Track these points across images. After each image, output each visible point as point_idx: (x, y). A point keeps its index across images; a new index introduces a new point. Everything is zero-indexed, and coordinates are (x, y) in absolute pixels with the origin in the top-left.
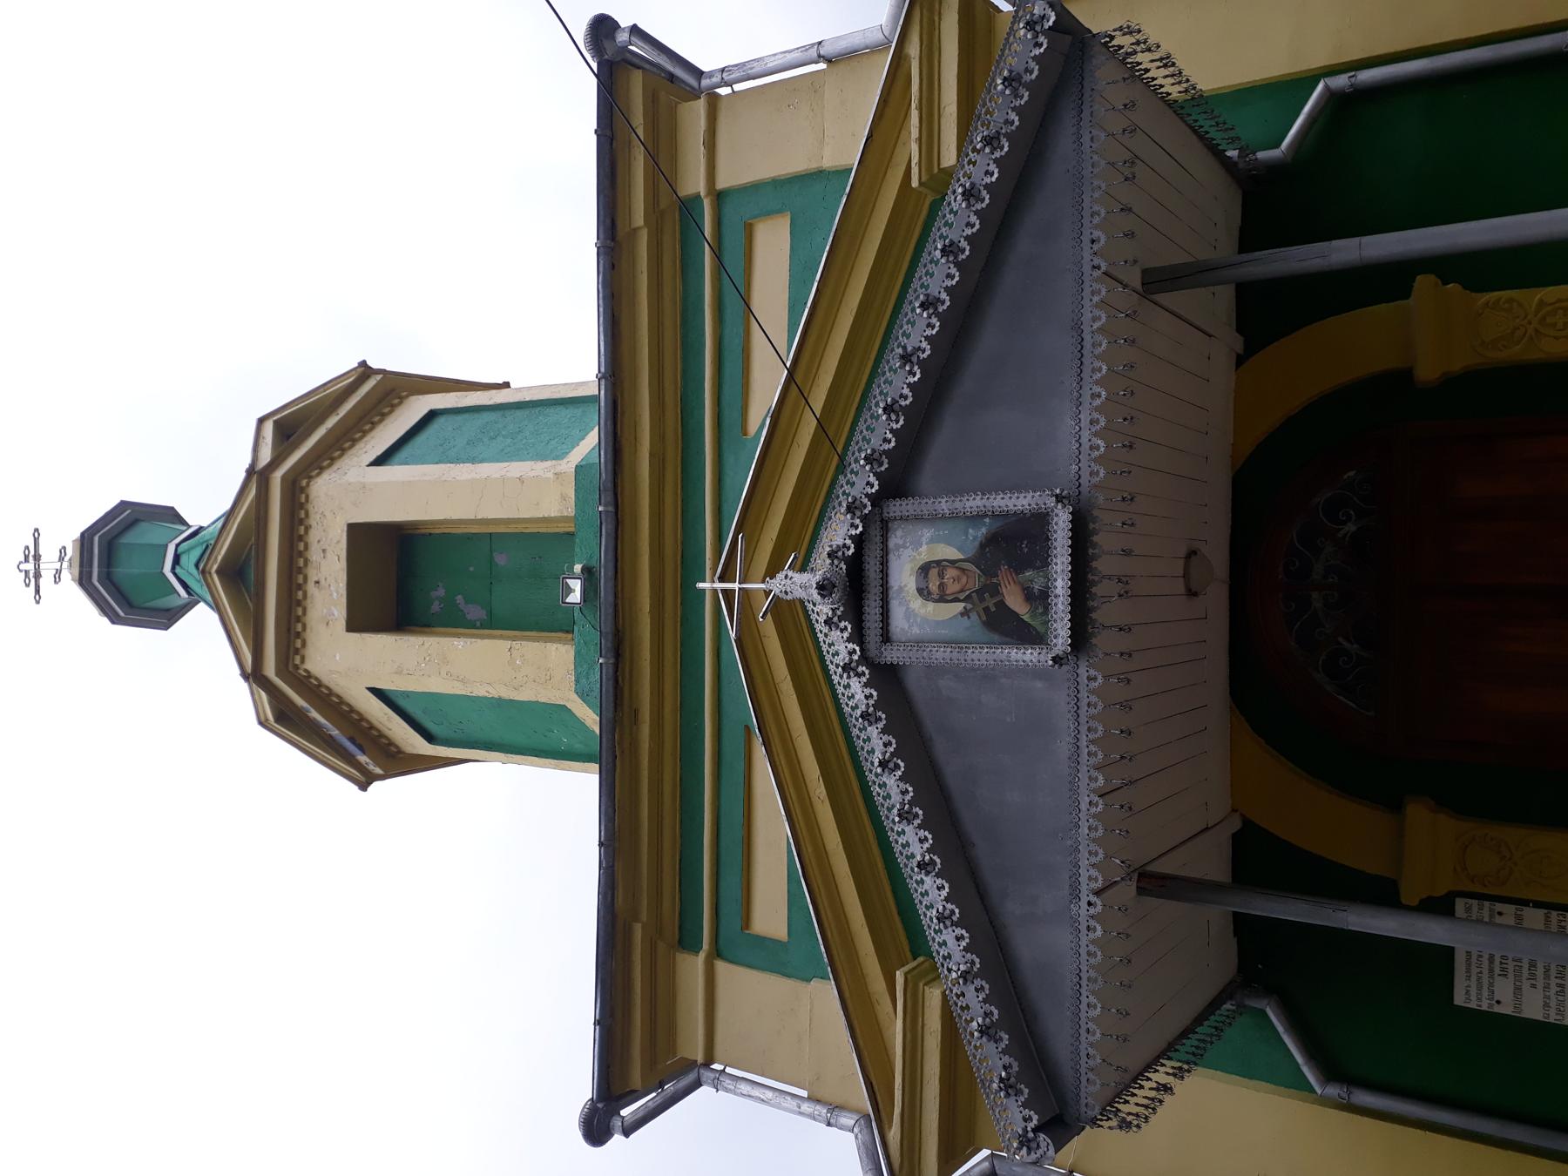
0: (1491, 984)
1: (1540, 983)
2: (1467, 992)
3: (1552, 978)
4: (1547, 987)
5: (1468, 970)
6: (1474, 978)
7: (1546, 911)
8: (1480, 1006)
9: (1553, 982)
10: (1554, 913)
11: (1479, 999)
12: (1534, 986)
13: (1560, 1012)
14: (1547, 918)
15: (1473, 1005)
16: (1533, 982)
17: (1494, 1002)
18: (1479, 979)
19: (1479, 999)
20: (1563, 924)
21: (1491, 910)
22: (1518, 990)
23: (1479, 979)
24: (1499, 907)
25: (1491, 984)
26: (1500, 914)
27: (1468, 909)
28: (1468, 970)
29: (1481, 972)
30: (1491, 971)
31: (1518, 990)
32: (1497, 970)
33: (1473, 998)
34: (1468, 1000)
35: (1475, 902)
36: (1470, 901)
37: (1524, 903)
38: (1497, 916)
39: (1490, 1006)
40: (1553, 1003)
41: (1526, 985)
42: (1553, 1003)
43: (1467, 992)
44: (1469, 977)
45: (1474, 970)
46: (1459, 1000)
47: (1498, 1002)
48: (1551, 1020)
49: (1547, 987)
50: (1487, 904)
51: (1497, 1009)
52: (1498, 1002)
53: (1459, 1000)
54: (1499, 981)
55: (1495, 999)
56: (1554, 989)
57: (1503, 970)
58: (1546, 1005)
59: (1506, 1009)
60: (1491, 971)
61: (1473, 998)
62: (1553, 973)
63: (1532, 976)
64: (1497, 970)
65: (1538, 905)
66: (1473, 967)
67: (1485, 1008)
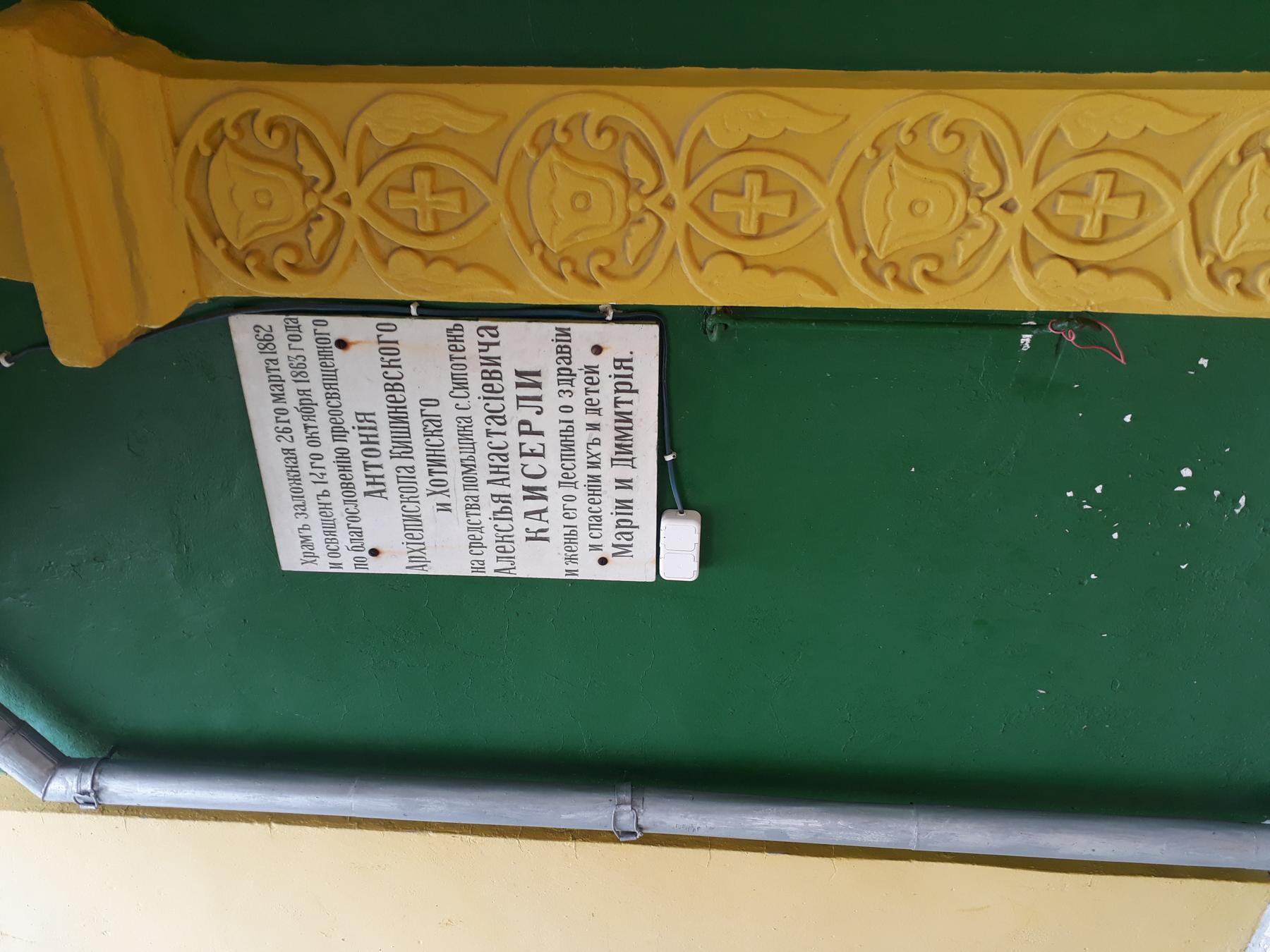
0: (353, 517)
1: (457, 497)
2: (305, 541)
3: (482, 483)
4: (472, 506)
5: (297, 493)
6: (313, 509)
7: (450, 323)
8: (339, 565)
9: (485, 491)
10: (470, 327)
11: (334, 553)
12: (444, 507)
13: (504, 552)
14: (454, 339)
15: (322, 565)
16: (441, 499)
17: (366, 554)
18: (324, 509)
19: (334, 553)
20: (493, 352)
21: (321, 339)
22: (412, 520)
23: (324, 509)
24: (338, 326)
25: (353, 517)
26: (342, 344)
27: (266, 342)
28: (297, 493)
29: (325, 494)
30: (347, 486)
31: (412, 520)
32: (361, 485)
33: (320, 548)
34: (310, 555)
35: (276, 322)
36: (265, 320)
37: (398, 309)
38: (337, 352)
39: (359, 562)
40: (489, 537)
41: (427, 506)
42: (489, 537)
43: (305, 541)
44: (301, 509)
45: (311, 491)
46: (291, 559)
47: (374, 552)
48: (489, 572)
49: (472, 506)
50: (306, 321)
51: (375, 567)
52: (374, 552)
53: (291, 559)
54: (366, 504)
55: (368, 546)
56: (488, 508)
57: (373, 480)
58: (475, 544)
59: (393, 564)
60: (347, 486)
61: (320, 548)
62: (483, 473)
63: (439, 487)
64: (361, 485)
65: (430, 310)
66: (306, 482)
67: (348, 567)
